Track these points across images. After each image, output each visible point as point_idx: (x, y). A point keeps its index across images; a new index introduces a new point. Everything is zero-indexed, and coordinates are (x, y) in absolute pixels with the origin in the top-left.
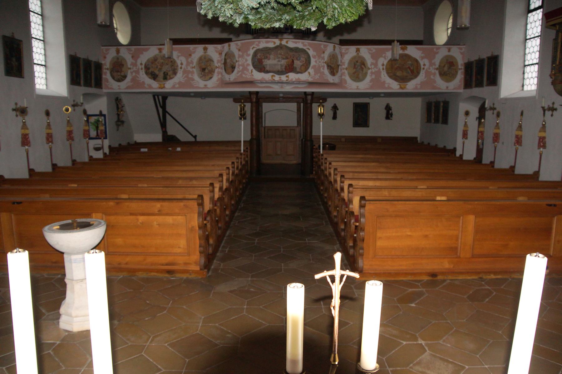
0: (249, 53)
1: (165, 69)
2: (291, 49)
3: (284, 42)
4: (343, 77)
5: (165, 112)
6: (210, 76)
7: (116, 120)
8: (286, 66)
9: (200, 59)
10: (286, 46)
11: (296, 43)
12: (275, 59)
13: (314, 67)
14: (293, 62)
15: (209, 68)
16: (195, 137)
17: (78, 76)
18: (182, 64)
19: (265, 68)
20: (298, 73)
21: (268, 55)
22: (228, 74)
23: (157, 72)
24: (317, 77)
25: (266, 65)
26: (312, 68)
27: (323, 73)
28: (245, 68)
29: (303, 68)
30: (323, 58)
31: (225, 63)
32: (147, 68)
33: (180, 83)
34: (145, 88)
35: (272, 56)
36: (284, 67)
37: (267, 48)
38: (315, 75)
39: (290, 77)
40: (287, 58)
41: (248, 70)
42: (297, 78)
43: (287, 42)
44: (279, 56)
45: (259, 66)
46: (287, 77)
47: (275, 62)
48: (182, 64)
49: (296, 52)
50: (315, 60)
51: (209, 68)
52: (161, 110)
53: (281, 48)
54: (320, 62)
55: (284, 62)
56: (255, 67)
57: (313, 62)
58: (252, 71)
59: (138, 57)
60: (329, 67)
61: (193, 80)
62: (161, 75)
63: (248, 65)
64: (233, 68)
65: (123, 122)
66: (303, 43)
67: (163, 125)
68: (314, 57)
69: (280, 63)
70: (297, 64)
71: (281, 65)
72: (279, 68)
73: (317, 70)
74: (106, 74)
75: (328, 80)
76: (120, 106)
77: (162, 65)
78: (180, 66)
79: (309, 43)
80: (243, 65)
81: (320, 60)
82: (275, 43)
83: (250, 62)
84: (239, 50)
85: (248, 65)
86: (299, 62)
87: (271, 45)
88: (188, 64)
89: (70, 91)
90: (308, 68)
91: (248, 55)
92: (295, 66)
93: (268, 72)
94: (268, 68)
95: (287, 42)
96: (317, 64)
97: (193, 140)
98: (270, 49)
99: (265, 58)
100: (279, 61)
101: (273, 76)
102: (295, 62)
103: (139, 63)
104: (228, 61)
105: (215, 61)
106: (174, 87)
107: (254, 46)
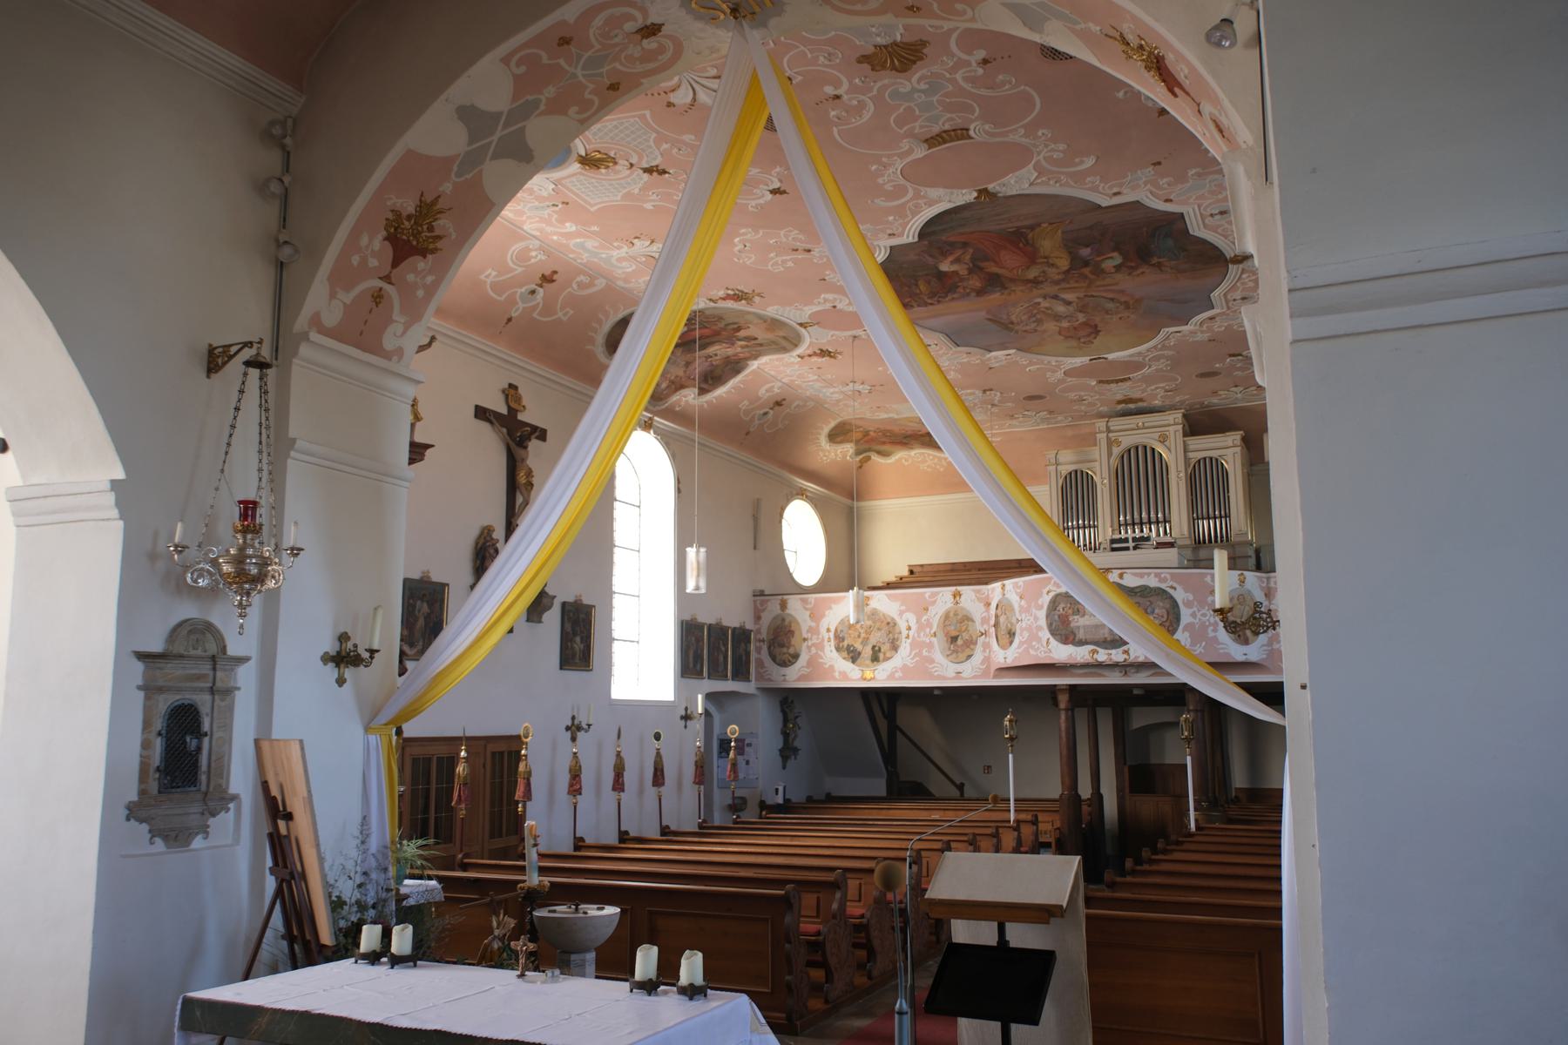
1: (873, 641)
4: (1276, 646)
5: (893, 728)
6: (968, 652)
7: (781, 745)
9: (947, 616)
11: (1141, 576)
13: (1189, 627)
15: (966, 636)
16: (961, 787)
17: (698, 658)
18: (909, 628)
22: (1003, 648)
23: (859, 646)
27: (1215, 639)
28: (1034, 637)
31: (996, 625)
32: (839, 638)
33: (905, 668)
34: (834, 679)
38: (1193, 644)
41: (1039, 640)
43: (1121, 576)
45: (1063, 630)
46: (1126, 652)
48: (909, 628)
51: (966, 636)
52: (883, 725)
54: (1204, 615)
57: (1186, 617)
59: (823, 616)
61: (932, 661)
62: (867, 652)
64: (1012, 634)
65: (796, 750)
66: (1157, 575)
67: (890, 756)
68: (1188, 604)
74: (759, 650)
75: (1228, 655)
76: (791, 716)
77: (869, 631)
78: (905, 632)
80: (1029, 629)
83: (1043, 622)
85: (1040, 628)
88: (921, 628)
89: (678, 689)
91: (1041, 607)
93: (1081, 643)
94: (1081, 635)
95: (1121, 576)
97: (955, 793)
101: (1094, 652)
103: (823, 631)
104: (1002, 619)
105: (977, 619)
106: (891, 677)
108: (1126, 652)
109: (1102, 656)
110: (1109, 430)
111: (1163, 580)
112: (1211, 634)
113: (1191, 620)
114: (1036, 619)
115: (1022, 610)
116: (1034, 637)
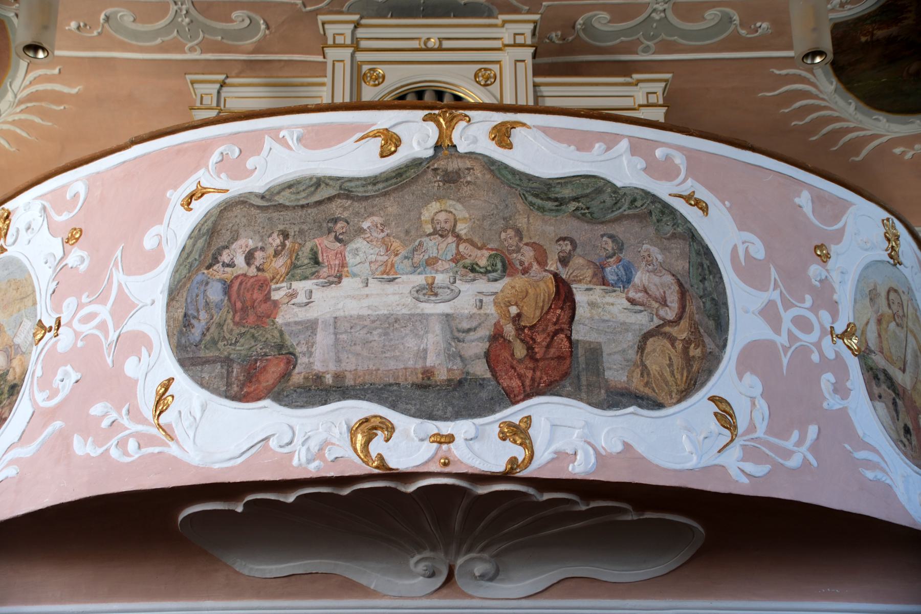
0: (149, 242)
2: (544, 193)
3: (473, 135)
8: (497, 337)
10: (491, 165)
11: (583, 142)
12: (388, 275)
13: (757, 357)
14: (564, 295)
19: (291, 359)
20: (616, 399)
21: (326, 243)
24: (798, 450)
25: (311, 326)
26: (745, 364)
28: (102, 378)
29: (660, 357)
30: (824, 297)
35: (362, 253)
36: (476, 346)
37: (319, 182)
38: (779, 425)
39: (539, 433)
40: (503, 265)
41: (122, 391)
42: (610, 444)
43: (502, 136)
44: (432, 246)
45: (235, 348)
46: (518, 432)
47: (396, 297)
49: (586, 216)
50: (759, 299)
53: (452, 179)
55: (475, 300)
56: (190, 357)
57: (745, 322)
58: (161, 402)
60: (876, 377)
63: (135, 343)
68: (752, 273)
69: (431, 308)
70: (605, 315)
71: (455, 330)
72: (429, 351)
73: (792, 398)
79: (691, 155)
80: (86, 354)
81: (803, 309)
82: (390, 141)
84: (73, 238)
85: (135, 343)
86: (616, 305)
87: (357, 159)
90: (711, 362)
92: (580, 333)
93: (319, 391)
95: (502, 136)
96: (782, 340)
98: (346, 190)
99: (293, 272)
100: (430, 291)
101: (371, 427)
102: (580, 297)
107: (205, 177)
108: (518, 432)
109: (410, 446)
110: (356, 46)
111: (665, 171)
112: (833, 402)
113: (763, 331)
114: (124, 307)
115: (66, 282)
116: (102, 378)
